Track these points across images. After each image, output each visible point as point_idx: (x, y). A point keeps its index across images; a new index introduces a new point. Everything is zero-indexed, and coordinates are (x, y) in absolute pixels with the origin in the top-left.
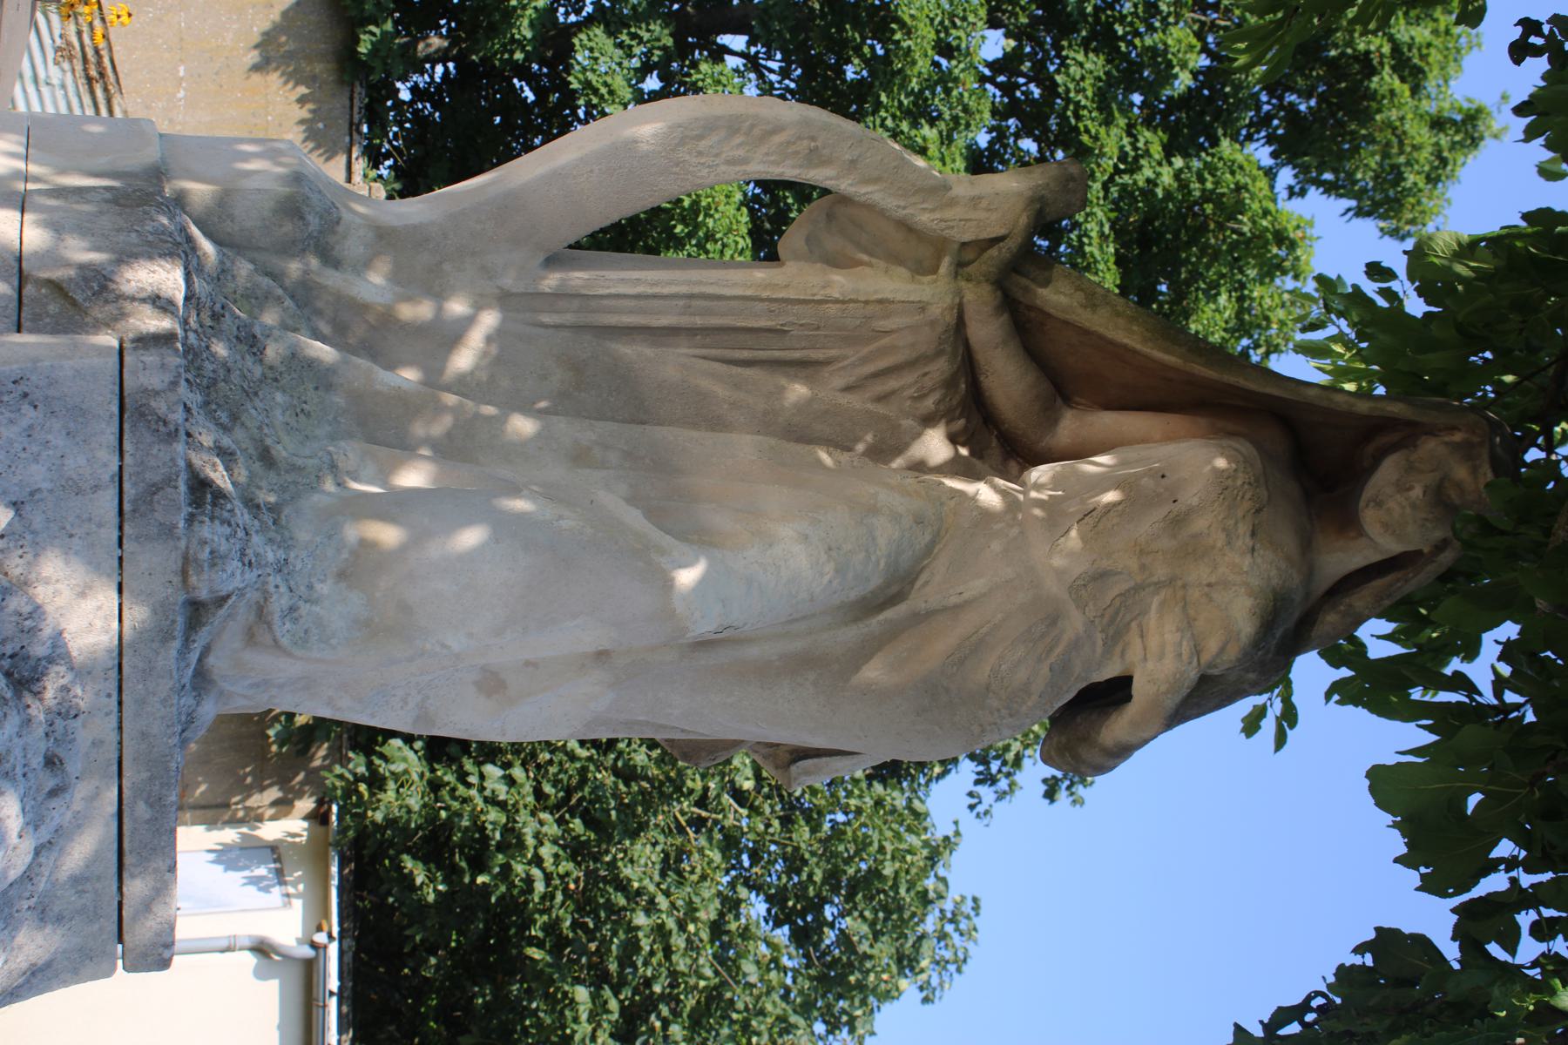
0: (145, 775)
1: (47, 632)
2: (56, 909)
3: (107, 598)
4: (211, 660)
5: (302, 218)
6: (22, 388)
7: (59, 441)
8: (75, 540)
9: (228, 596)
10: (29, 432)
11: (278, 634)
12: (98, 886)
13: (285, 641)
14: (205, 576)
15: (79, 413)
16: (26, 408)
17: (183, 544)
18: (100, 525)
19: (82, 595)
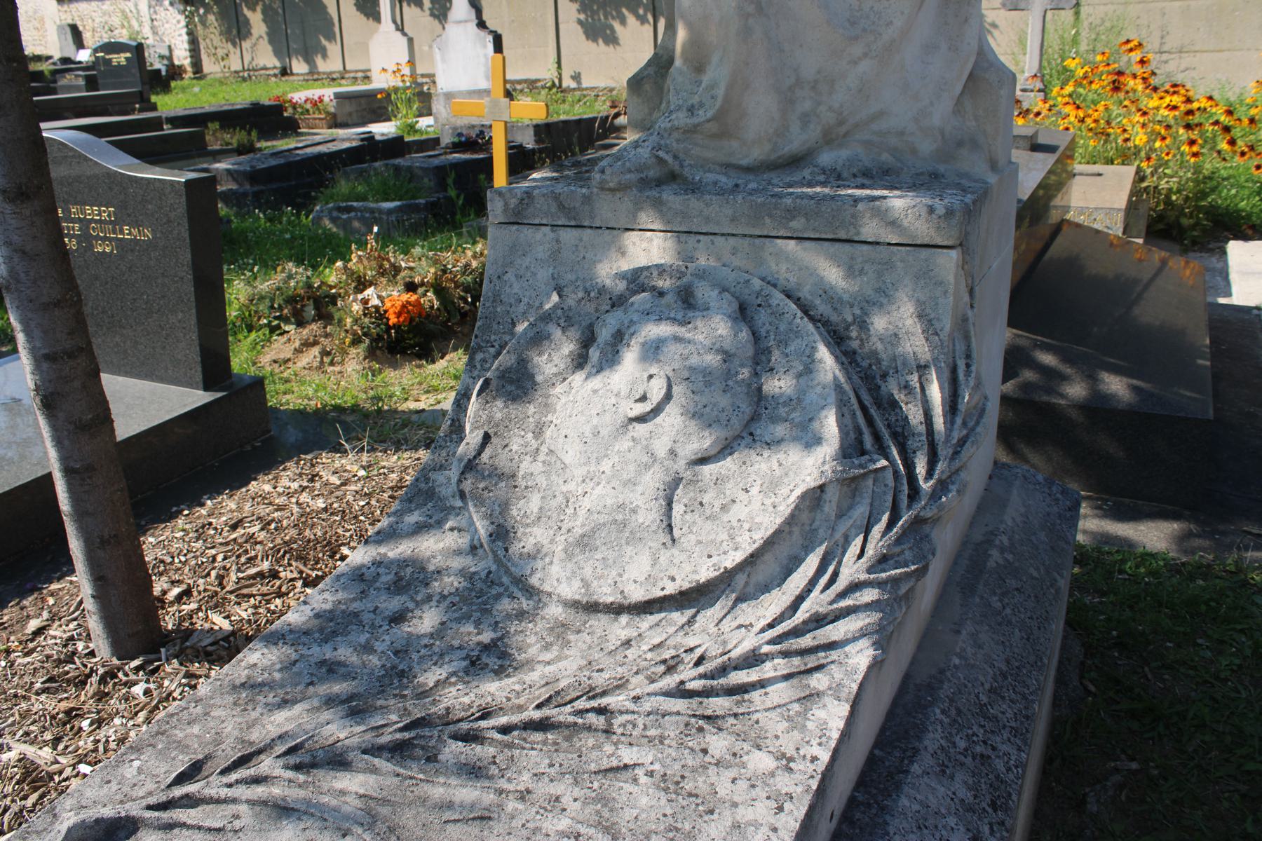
0: (767, 220)
1: (608, 282)
2: (870, 292)
3: (633, 236)
4: (744, 162)
5: (642, 79)
6: (495, 279)
7: (527, 261)
8: (587, 256)
9: (657, 157)
10: (519, 277)
11: (703, 119)
12: (859, 260)
13: (709, 114)
14: (608, 178)
15: (513, 248)
16: (505, 278)
17: (595, 190)
18: (581, 240)
19: (623, 254)
